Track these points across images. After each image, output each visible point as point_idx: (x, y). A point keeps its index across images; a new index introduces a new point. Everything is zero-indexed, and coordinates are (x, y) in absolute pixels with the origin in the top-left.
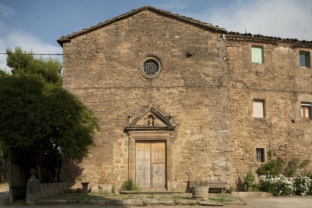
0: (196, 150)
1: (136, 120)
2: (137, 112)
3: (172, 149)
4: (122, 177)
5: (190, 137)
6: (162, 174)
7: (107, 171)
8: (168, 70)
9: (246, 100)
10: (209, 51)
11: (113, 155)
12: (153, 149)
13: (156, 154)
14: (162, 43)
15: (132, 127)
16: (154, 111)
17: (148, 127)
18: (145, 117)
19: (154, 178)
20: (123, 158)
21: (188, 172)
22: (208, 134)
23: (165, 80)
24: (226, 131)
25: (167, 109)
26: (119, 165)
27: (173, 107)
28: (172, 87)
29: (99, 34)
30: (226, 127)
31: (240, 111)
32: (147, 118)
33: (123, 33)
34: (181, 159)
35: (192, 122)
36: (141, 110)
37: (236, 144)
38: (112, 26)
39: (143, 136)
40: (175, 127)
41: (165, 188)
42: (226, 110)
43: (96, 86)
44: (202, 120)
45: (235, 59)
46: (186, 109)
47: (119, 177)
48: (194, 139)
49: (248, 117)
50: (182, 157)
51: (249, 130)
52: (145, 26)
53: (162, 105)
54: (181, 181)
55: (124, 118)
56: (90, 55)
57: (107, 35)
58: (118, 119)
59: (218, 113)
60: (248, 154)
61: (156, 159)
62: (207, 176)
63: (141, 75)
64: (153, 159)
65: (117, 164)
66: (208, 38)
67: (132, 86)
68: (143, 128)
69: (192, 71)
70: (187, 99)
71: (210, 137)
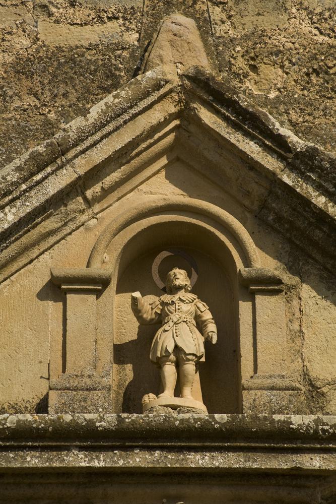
16: (251, 148)
32: (107, 265)
68: (33, 460)
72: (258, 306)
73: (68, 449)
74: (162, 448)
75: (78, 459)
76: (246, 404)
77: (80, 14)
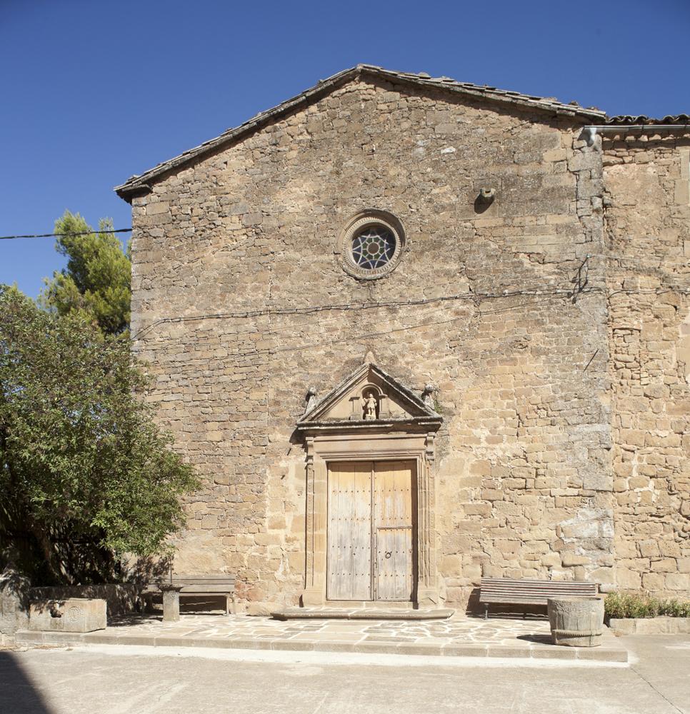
0: (509, 484)
1: (326, 404)
2: (332, 379)
3: (431, 486)
4: (288, 570)
5: (486, 448)
6: (403, 562)
7: (248, 552)
8: (422, 252)
9: (668, 329)
10: (547, 185)
11: (264, 506)
12: (378, 487)
13: (389, 501)
14: (405, 172)
15: (315, 425)
18: (351, 394)
19: (382, 573)
20: (292, 513)
21: (481, 553)
22: (543, 439)
23: (411, 282)
24: (598, 427)
25: (418, 368)
26: (281, 534)
27: (437, 361)
28: (434, 301)
29: (226, 163)
30: (599, 416)
31: (650, 365)
33: (294, 154)
34: (460, 516)
35: (492, 404)
36: (343, 374)
37: (636, 466)
38: (262, 138)
39: (349, 449)
40: (440, 420)
41: (410, 601)
42: (600, 362)
43: (219, 312)
44: (523, 397)
45: (633, 203)
46: (474, 363)
47: (281, 570)
48: (500, 454)
49: (676, 383)
50: (462, 510)
51: (678, 422)
52: (355, 126)
53: (403, 356)
54: (459, 581)
55: (297, 396)
56: (202, 224)
57: (250, 162)
58: (277, 403)
59: (575, 372)
60: (674, 498)
61: (387, 516)
62: (539, 568)
63: (343, 272)
64: (378, 516)
65: (276, 530)
66: (540, 142)
67: (318, 305)
68: (348, 427)
69: (494, 250)
70: (477, 336)
71: (550, 448)
75: (354, 427)
77: (356, 352)
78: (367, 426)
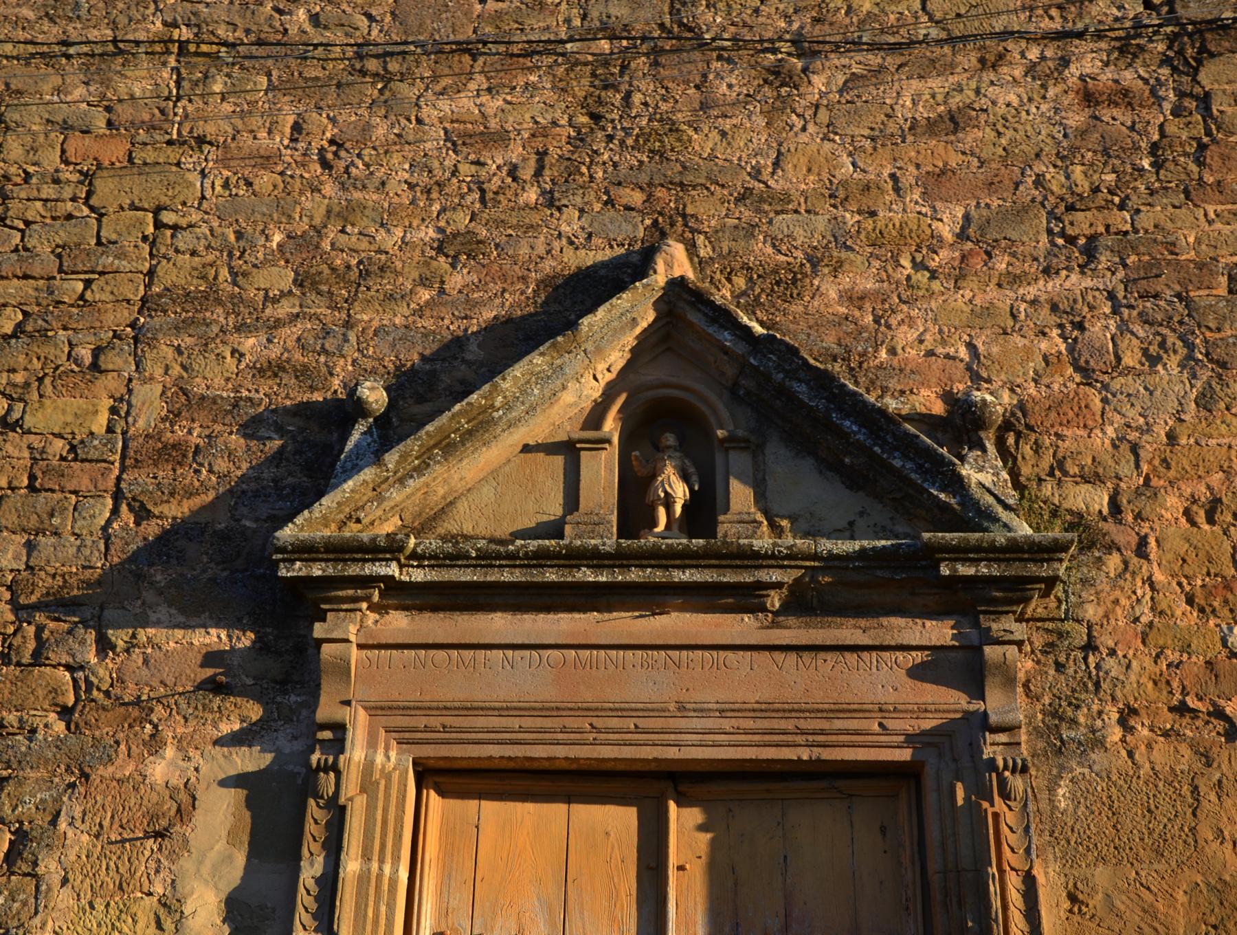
17: (620, 559)
40: (1053, 550)
68: (551, 576)
72: (731, 461)
73: (578, 567)
74: (652, 567)
76: (720, 535)
78: (659, 576)
